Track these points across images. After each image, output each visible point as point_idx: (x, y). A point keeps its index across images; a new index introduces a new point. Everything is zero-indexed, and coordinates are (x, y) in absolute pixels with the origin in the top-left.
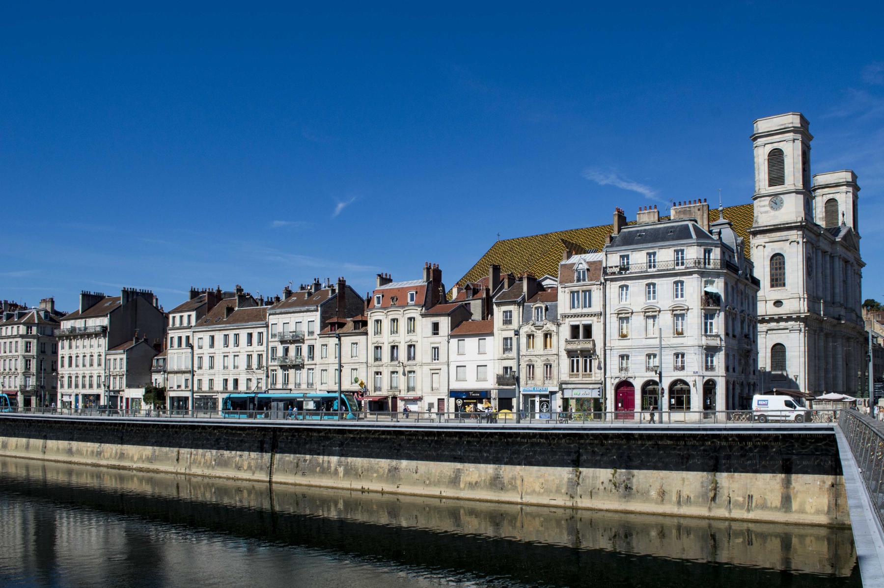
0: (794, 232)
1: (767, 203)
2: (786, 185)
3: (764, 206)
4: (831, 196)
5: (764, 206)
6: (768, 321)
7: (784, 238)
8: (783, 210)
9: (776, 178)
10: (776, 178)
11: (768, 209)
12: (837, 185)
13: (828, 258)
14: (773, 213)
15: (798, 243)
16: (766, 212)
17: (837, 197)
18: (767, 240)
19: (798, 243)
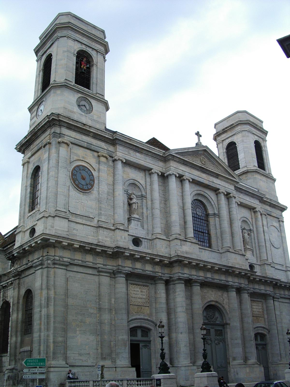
13: (155, 177)
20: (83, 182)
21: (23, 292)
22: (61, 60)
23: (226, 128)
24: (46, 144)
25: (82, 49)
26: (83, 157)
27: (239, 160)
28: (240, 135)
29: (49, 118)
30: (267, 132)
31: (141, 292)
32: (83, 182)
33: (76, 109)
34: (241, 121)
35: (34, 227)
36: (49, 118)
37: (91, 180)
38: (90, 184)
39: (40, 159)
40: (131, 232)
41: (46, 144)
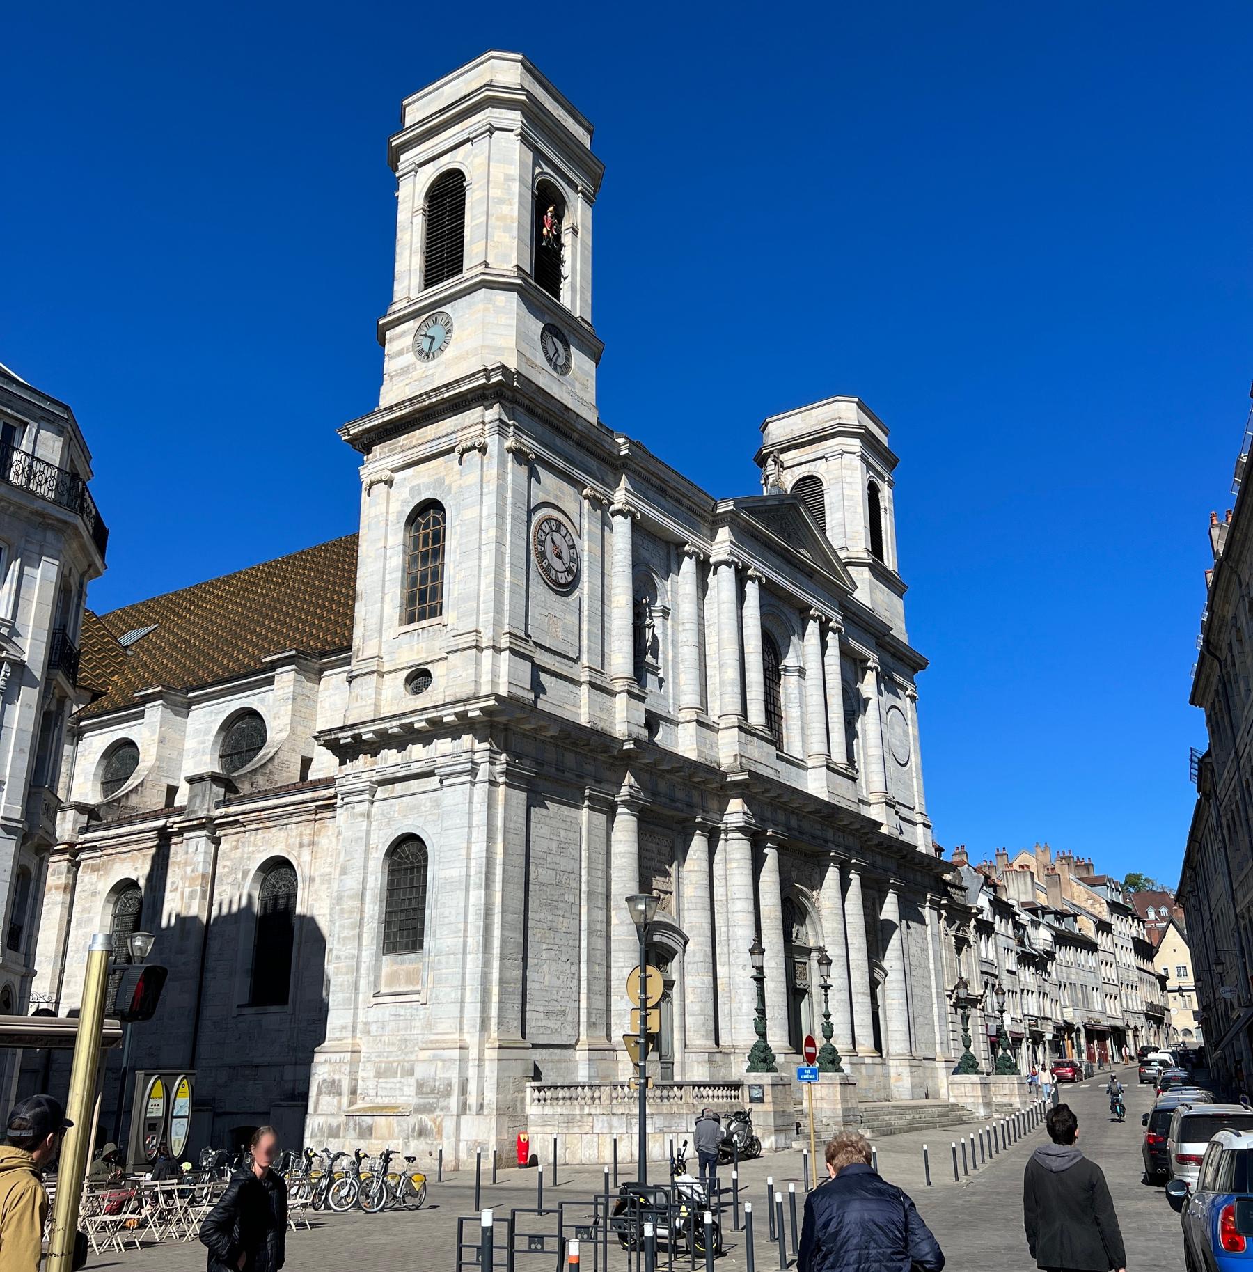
0: (476, 413)
1: (408, 340)
2: (466, 274)
3: (401, 353)
4: (803, 471)
5: (401, 353)
6: (373, 748)
7: (445, 447)
8: (450, 352)
9: (444, 255)
10: (444, 255)
11: (410, 358)
12: (819, 437)
14: (422, 367)
15: (483, 449)
16: (405, 371)
17: (819, 469)
18: (398, 460)
19: (483, 449)
20: (558, 564)
21: (382, 839)
22: (501, 201)
23: (800, 437)
24: (472, 448)
25: (546, 177)
26: (557, 497)
27: (827, 527)
28: (834, 463)
29: (488, 379)
30: (897, 461)
31: (659, 853)
32: (558, 564)
33: (540, 359)
34: (844, 425)
35: (428, 667)
36: (488, 379)
37: (572, 560)
38: (569, 571)
39: (439, 482)
40: (652, 703)
41: (472, 448)
